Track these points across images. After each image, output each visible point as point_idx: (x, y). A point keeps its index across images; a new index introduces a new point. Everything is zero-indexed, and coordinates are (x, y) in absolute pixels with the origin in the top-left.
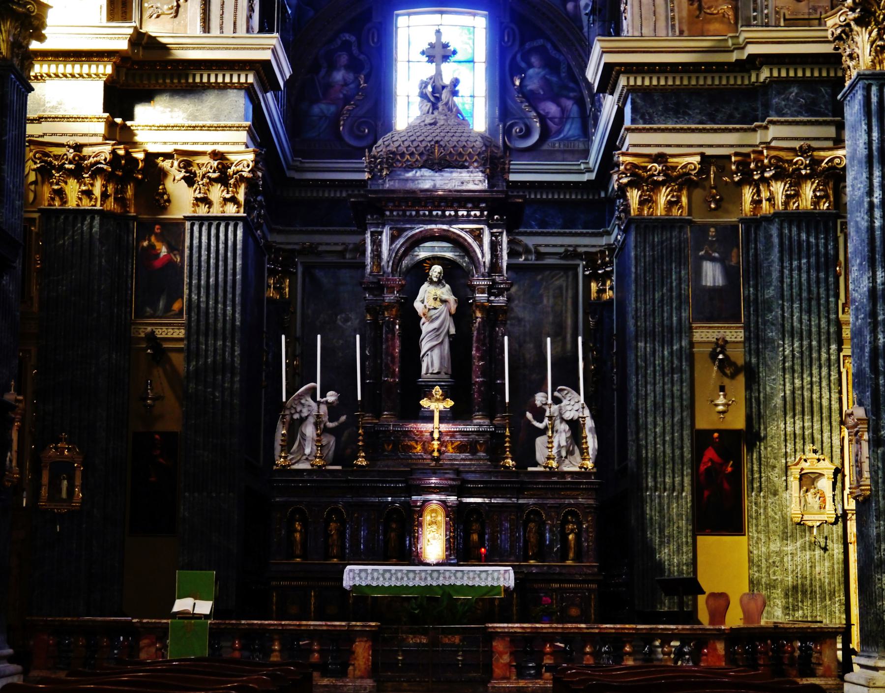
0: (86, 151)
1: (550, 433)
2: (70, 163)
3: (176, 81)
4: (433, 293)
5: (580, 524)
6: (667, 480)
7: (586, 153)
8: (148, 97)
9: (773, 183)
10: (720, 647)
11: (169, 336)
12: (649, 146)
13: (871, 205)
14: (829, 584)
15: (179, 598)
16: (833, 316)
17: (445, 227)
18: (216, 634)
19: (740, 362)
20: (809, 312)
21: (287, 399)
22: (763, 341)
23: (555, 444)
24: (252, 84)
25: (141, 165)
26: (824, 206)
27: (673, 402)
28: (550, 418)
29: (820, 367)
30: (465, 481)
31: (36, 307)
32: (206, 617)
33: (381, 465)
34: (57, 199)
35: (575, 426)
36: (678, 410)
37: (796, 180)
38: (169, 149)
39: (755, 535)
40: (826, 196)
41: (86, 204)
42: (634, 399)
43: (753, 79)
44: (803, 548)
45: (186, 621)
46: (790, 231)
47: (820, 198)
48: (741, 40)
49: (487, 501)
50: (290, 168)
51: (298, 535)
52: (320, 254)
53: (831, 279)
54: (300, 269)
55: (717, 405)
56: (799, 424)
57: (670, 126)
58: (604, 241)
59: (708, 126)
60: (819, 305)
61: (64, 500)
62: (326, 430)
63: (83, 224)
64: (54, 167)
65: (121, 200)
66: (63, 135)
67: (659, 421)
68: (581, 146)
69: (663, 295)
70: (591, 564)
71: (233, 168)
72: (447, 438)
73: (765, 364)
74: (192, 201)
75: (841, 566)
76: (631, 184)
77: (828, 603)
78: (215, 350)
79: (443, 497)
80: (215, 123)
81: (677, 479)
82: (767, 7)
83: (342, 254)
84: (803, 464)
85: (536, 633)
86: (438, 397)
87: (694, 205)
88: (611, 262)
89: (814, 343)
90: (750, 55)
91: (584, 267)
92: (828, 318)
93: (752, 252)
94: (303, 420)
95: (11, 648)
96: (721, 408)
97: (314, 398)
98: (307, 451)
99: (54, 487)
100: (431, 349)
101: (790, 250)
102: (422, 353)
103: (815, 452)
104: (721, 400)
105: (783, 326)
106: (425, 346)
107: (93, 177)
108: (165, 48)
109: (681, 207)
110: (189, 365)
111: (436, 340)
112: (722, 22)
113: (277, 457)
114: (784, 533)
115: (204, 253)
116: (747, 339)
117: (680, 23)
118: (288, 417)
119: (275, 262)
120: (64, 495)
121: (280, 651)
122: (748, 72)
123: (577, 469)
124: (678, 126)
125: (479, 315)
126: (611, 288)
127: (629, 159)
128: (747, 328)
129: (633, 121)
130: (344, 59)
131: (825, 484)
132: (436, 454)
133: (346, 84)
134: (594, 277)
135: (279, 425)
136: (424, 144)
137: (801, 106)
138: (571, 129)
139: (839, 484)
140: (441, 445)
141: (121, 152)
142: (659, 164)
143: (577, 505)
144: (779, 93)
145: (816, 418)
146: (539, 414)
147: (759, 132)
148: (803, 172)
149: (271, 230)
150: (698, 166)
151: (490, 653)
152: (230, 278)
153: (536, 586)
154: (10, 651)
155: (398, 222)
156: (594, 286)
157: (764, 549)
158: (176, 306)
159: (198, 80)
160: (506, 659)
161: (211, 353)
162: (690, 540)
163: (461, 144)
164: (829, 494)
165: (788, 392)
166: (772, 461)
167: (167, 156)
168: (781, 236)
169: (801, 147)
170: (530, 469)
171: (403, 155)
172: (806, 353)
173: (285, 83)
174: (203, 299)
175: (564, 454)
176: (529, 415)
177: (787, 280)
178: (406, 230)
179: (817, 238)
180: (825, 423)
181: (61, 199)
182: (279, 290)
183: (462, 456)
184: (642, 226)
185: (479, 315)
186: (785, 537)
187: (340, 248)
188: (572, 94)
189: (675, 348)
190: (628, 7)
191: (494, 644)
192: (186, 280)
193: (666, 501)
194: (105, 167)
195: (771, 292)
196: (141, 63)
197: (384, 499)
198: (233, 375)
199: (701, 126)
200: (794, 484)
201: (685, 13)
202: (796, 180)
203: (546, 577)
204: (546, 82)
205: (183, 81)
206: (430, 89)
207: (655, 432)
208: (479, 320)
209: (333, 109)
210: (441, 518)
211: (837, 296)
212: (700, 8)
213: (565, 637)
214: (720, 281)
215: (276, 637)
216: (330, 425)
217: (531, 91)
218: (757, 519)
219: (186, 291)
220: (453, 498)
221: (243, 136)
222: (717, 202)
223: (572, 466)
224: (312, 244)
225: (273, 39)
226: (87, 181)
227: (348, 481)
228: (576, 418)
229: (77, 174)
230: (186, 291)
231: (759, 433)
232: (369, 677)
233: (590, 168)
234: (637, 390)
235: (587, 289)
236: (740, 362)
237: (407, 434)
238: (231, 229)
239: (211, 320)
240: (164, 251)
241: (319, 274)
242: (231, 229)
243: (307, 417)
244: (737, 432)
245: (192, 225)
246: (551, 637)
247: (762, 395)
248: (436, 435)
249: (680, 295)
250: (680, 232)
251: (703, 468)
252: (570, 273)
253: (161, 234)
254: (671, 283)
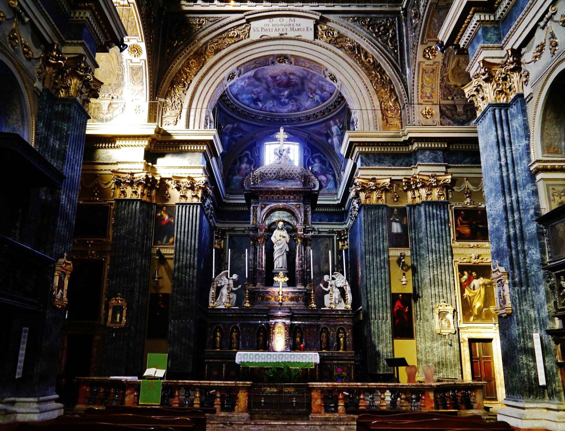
0: (135, 176)
1: (331, 292)
2: (129, 180)
3: (174, 149)
5: (345, 333)
6: (380, 315)
7: (337, 194)
8: (163, 155)
9: (421, 190)
10: (431, 395)
11: (168, 253)
12: (368, 175)
13: (501, 166)
14: (454, 361)
15: (148, 368)
16: (449, 244)
17: (285, 204)
18: (165, 387)
19: (410, 264)
20: (439, 242)
21: (215, 277)
22: (419, 255)
23: (333, 297)
24: (205, 150)
25: (158, 182)
26: (442, 199)
27: (382, 281)
28: (331, 285)
29: (445, 266)
30: (293, 314)
31: (111, 240)
32: (161, 378)
33: (256, 307)
34: (122, 194)
35: (342, 290)
36: (384, 284)
37: (431, 187)
38: (170, 176)
39: (419, 339)
40: (443, 195)
41: (134, 197)
42: (365, 280)
43: (410, 148)
44: (441, 345)
45: (150, 381)
46: (429, 209)
47: (441, 195)
48: (406, 132)
49: (304, 323)
50: (224, 198)
51: (218, 338)
52: (235, 231)
53: (447, 229)
54: (228, 237)
55: (402, 282)
56: (437, 290)
57: (377, 167)
58: (344, 227)
59: (393, 167)
60: (443, 239)
61: (118, 323)
62: (232, 291)
63: (132, 205)
64: (122, 182)
65: (149, 196)
66: (126, 169)
67: (376, 290)
68: (335, 192)
69: (376, 236)
70: (350, 352)
71: (197, 183)
72: (286, 295)
73: (421, 265)
74: (179, 196)
75: (458, 353)
76: (361, 190)
77: (453, 369)
78: (187, 259)
79: (284, 321)
80: (190, 165)
81: (385, 315)
82: (414, 121)
83: (244, 231)
84: (440, 308)
85: (334, 388)
87: (387, 199)
88: (347, 234)
89: (442, 256)
90: (410, 138)
91: (336, 236)
92: (447, 245)
93: (412, 218)
94: (222, 287)
95: (57, 394)
96: (404, 283)
97: (227, 277)
98: (224, 300)
99: (114, 317)
100: (279, 257)
101: (429, 217)
103: (444, 302)
104: (404, 279)
105: (428, 248)
106: (276, 256)
107: (138, 185)
108: (169, 135)
109: (383, 200)
110: (175, 265)
112: (396, 128)
113: (210, 303)
114: (433, 338)
115: (183, 218)
116: (412, 254)
117: (379, 128)
118: (215, 286)
119: (218, 233)
120: (118, 320)
121: (199, 397)
122: (408, 146)
123: (344, 309)
124: (380, 167)
125: (299, 241)
126: (347, 244)
127: (361, 180)
128: (412, 250)
129: (362, 165)
130: (246, 160)
131: (450, 316)
132: (280, 301)
133: (246, 169)
134: (341, 240)
135: (212, 288)
136: (276, 170)
137: (431, 159)
138: (331, 185)
139: (455, 316)
140: (283, 297)
141: (150, 176)
142: (373, 182)
143: (344, 325)
144: (421, 154)
145: (444, 287)
146: (326, 285)
147: (414, 169)
148: (434, 185)
149: (217, 222)
150: (389, 183)
151: (310, 398)
152: (194, 228)
153: (326, 362)
154: (57, 396)
155: (265, 201)
156: (340, 244)
157: (423, 346)
158: (171, 240)
159: (183, 148)
160: (319, 402)
161: (185, 260)
162: (391, 341)
163: (291, 170)
164: (451, 320)
165: (432, 277)
166: (425, 307)
167: (170, 179)
168: (425, 211)
169: (432, 175)
170: (322, 308)
171: (267, 174)
172: (438, 260)
173: (221, 154)
174: (182, 237)
175: (337, 302)
176: (321, 285)
177: (429, 229)
178: (268, 205)
179: (440, 212)
180: (448, 290)
181: (124, 195)
182: (220, 245)
183: (292, 302)
184: (367, 207)
185: (299, 241)
186: (433, 340)
187: (243, 229)
188: (331, 173)
189: (382, 258)
190: (358, 122)
191: (312, 394)
192: (176, 229)
193: (380, 324)
194: (143, 182)
195: (421, 235)
196: (160, 142)
197: (256, 322)
198: (194, 269)
199: (389, 167)
200: (436, 316)
201: (381, 124)
202: (431, 187)
203: (331, 358)
204: (321, 168)
205: (177, 149)
206: (277, 152)
207: (375, 294)
208: (299, 243)
209: (241, 178)
210: (283, 330)
211: (450, 236)
212: (387, 122)
213: (349, 390)
214: (400, 231)
215: (197, 389)
216: (234, 289)
217: (316, 172)
218: (420, 332)
219: (175, 234)
220: (288, 322)
221: (201, 171)
222: (397, 198)
223: (342, 307)
224: (232, 228)
225: (214, 131)
226: (136, 187)
227: (241, 314)
228: (342, 286)
229: (131, 184)
230: (175, 234)
231: (419, 295)
232: (246, 412)
234: (366, 276)
235: (338, 245)
236: (410, 264)
237: (267, 292)
238: (195, 208)
239: (185, 246)
240: (166, 217)
241: (235, 239)
242: (195, 208)
243: (224, 285)
244: (410, 294)
245: (179, 207)
246: (341, 390)
247: (419, 278)
248: (281, 293)
249: (383, 236)
250: (382, 210)
251: (395, 310)
252: (331, 239)
253: (166, 210)
254: (379, 231)
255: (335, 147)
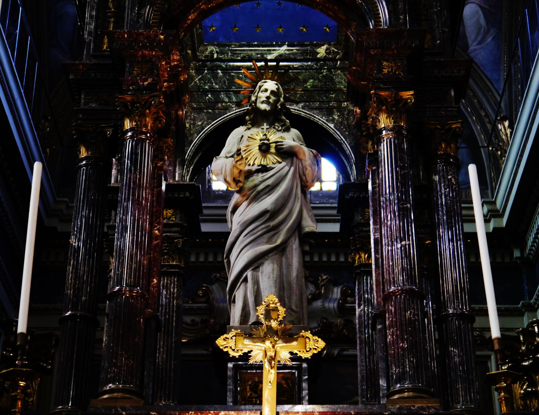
4: (261, 136)
86: (274, 324)
102: (231, 278)
111: (268, 242)
125: (384, 121)
185: (384, 121)
233: (498, 211)
255: (470, 41)
